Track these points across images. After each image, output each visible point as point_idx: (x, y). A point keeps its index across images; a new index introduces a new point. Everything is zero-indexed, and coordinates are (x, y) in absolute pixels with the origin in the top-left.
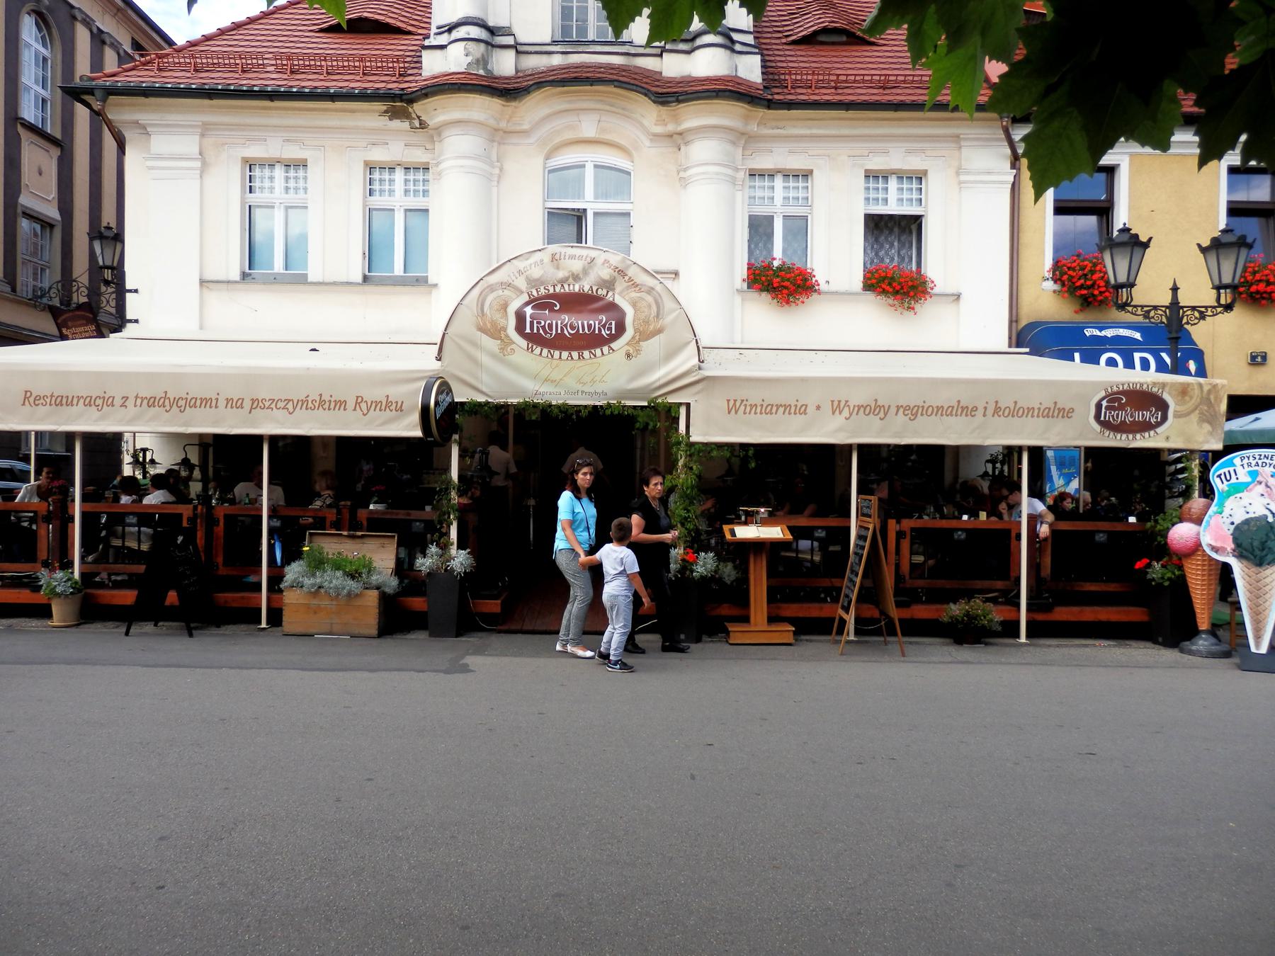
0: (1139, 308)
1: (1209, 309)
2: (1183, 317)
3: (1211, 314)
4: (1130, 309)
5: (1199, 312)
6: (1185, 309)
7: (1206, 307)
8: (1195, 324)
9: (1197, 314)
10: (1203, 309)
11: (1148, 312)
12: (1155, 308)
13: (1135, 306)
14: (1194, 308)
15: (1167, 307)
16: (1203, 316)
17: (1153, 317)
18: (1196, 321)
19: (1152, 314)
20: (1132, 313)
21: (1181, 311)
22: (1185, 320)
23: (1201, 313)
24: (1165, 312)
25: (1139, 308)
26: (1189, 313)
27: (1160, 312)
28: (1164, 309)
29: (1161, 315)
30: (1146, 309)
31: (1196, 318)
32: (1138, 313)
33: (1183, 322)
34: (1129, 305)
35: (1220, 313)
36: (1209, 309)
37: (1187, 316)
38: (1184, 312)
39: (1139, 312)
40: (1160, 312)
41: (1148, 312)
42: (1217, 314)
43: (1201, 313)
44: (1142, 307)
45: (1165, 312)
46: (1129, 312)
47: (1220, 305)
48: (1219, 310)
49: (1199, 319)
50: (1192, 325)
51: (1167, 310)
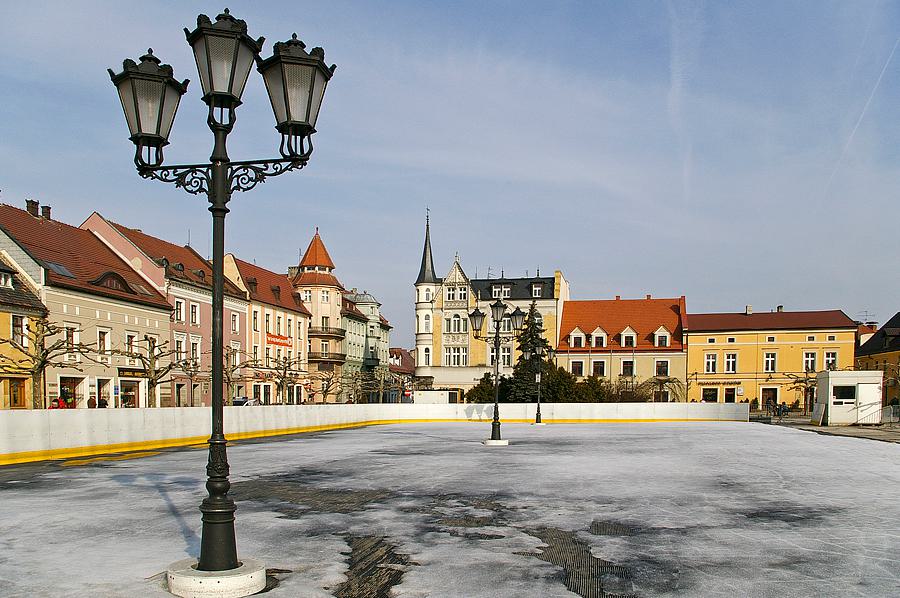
0: (171, 171)
1: (270, 165)
4: (158, 173)
5: (254, 169)
6: (235, 167)
7: (265, 162)
8: (249, 189)
9: (252, 174)
10: (261, 166)
11: (183, 176)
12: (193, 169)
13: (165, 169)
14: (246, 165)
16: (261, 176)
17: (190, 183)
18: (251, 184)
19: (188, 178)
20: (161, 179)
21: (229, 170)
22: (234, 184)
23: (257, 170)
24: (206, 174)
25: (171, 171)
26: (241, 172)
27: (200, 175)
28: (205, 170)
29: (202, 179)
30: (180, 171)
31: (250, 179)
34: (157, 167)
35: (286, 169)
36: (270, 165)
37: (238, 177)
38: (233, 172)
39: (171, 176)
40: (200, 175)
41: (183, 176)
42: (282, 172)
43: (257, 170)
44: (175, 168)
46: (157, 177)
47: (286, 159)
48: (285, 165)
50: (244, 190)
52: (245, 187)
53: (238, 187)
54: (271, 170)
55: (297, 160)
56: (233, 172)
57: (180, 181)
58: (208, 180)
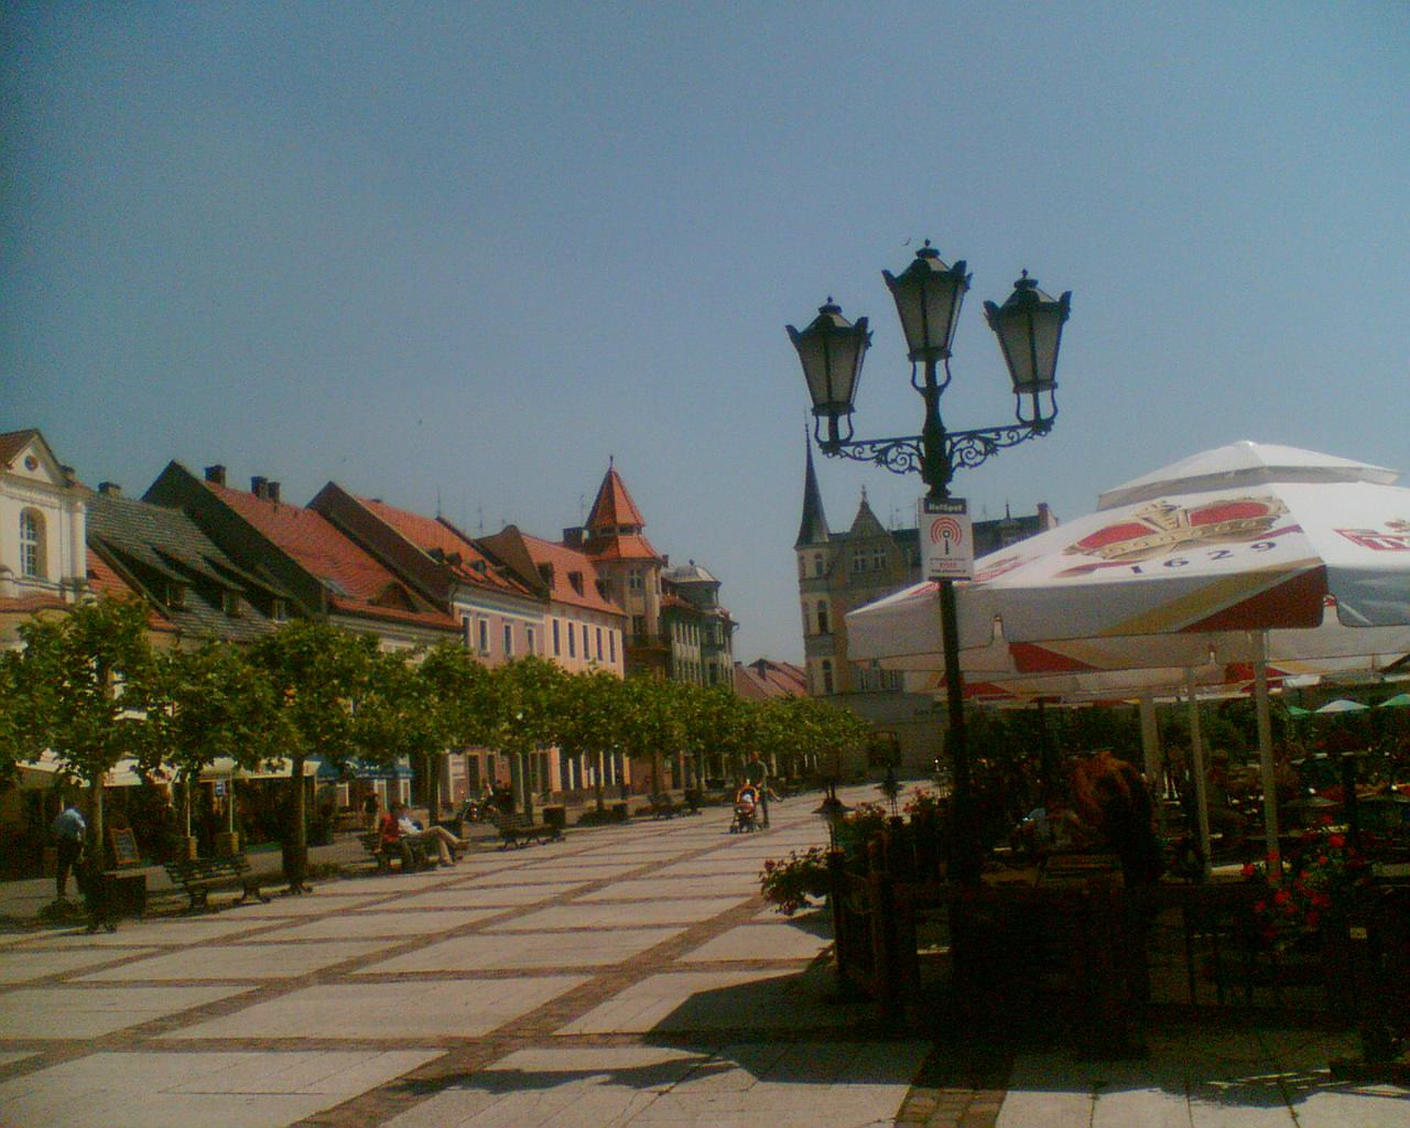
0: (867, 447)
2: (952, 452)
3: (1009, 441)
4: (849, 449)
5: (981, 439)
6: (955, 439)
7: (997, 431)
8: (976, 465)
9: (979, 445)
10: (992, 435)
11: (885, 451)
12: (898, 443)
13: (859, 444)
14: (971, 436)
15: (919, 439)
16: (991, 448)
17: (894, 461)
18: (979, 458)
19: (892, 454)
20: (854, 458)
21: (948, 444)
22: (956, 460)
23: (986, 442)
24: (917, 448)
25: (867, 447)
28: (914, 443)
29: (910, 455)
30: (879, 446)
31: (978, 453)
32: (863, 456)
33: (954, 465)
34: (847, 442)
35: (1026, 437)
36: (1004, 434)
37: (961, 450)
38: (953, 445)
39: (867, 453)
40: (910, 450)
41: (885, 451)
42: (1019, 441)
43: (986, 442)
44: (873, 443)
45: (917, 448)
46: (847, 455)
47: (1024, 424)
48: (1023, 432)
49: (986, 454)
50: (971, 466)
51: (922, 445)
52: (972, 462)
53: (962, 464)
54: (1004, 440)
55: (1040, 426)
56: (953, 445)
57: (881, 458)
58: (920, 455)
